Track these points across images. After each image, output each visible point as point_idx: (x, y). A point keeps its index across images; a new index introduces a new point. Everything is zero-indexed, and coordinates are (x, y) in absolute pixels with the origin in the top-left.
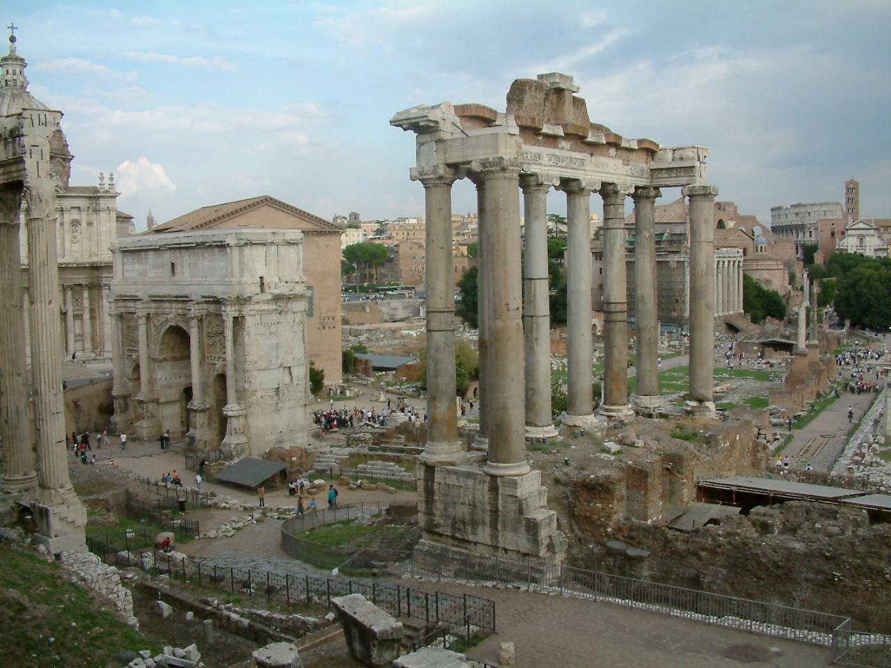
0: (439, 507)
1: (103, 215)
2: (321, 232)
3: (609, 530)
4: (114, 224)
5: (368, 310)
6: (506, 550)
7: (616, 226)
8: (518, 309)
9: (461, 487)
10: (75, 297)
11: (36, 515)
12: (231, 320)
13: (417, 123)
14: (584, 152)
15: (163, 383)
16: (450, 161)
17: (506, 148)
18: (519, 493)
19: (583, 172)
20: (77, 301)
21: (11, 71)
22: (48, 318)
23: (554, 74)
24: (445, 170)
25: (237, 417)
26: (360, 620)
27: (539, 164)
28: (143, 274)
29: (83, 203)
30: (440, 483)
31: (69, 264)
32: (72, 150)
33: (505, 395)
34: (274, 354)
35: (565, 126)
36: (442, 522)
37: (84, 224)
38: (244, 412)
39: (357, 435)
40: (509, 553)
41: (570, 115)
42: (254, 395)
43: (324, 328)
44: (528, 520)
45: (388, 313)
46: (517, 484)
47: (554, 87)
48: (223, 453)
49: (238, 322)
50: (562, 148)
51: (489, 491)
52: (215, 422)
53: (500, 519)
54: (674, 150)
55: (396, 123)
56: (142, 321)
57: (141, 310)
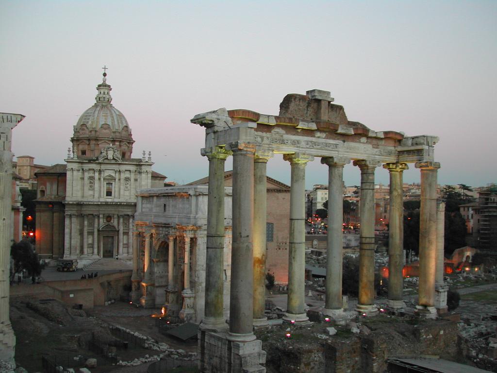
0: (207, 357)
1: (143, 175)
2: (280, 190)
4: (150, 181)
7: (367, 187)
10: (126, 222)
12: (189, 240)
14: (338, 139)
17: (246, 136)
18: (241, 353)
19: (337, 152)
20: (126, 225)
21: (102, 93)
23: (314, 90)
25: (190, 298)
27: (298, 147)
28: (151, 210)
29: (133, 168)
30: (207, 343)
32: (134, 137)
35: (318, 123)
36: (207, 367)
37: (132, 180)
38: (194, 295)
41: (325, 116)
42: (201, 285)
43: (280, 249)
44: (244, 370)
46: (239, 347)
47: (314, 98)
50: (319, 137)
51: (228, 350)
52: (180, 300)
54: (413, 138)
55: (193, 121)
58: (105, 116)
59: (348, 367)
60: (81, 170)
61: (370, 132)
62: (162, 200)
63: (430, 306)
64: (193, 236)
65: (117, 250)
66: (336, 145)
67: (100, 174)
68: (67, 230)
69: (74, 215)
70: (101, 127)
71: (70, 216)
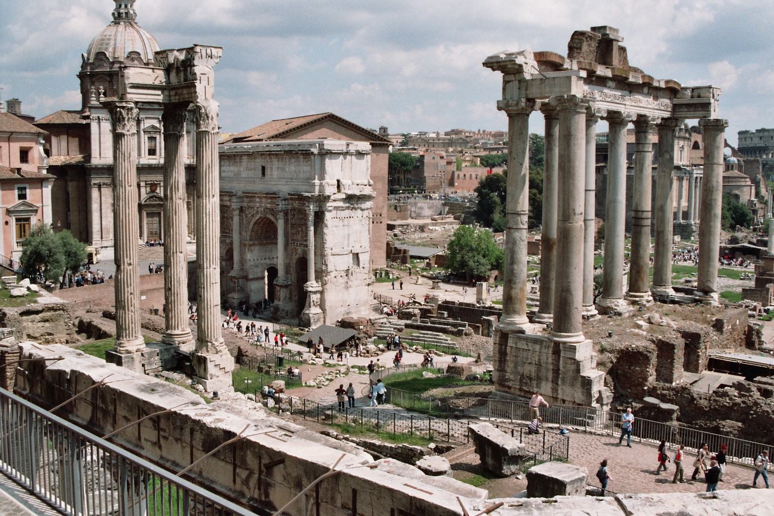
0: (510, 366)
3: (646, 388)
6: (564, 401)
8: (581, 214)
9: (529, 350)
11: (195, 362)
12: (312, 214)
14: (625, 90)
15: (252, 263)
16: (530, 96)
17: (577, 88)
18: (576, 358)
19: (624, 106)
24: (526, 103)
25: (315, 293)
26: (494, 441)
28: (238, 175)
30: (512, 347)
33: (569, 280)
34: (346, 242)
35: (613, 70)
36: (512, 377)
39: (408, 310)
40: (566, 402)
45: (415, 212)
48: (303, 321)
49: (319, 217)
51: (553, 354)
52: (295, 296)
53: (560, 376)
56: (237, 212)
57: (235, 204)
58: (132, 40)
62: (258, 160)
64: (317, 209)
68: (95, 206)
69: (104, 184)
71: (99, 187)
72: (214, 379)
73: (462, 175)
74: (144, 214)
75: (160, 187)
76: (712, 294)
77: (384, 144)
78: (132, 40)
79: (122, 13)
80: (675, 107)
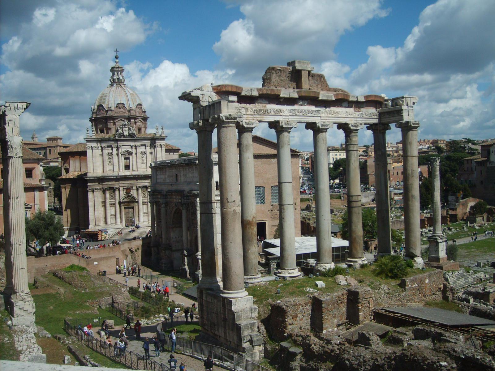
3: (286, 334)
5: (342, 198)
10: (144, 192)
13: (188, 98)
16: (205, 118)
19: (320, 118)
22: (16, 207)
27: (281, 115)
29: (148, 143)
30: (205, 300)
31: (139, 175)
33: (227, 251)
36: (207, 322)
44: (237, 324)
51: (222, 306)
55: (181, 98)
56: (163, 206)
59: (334, 317)
60: (100, 148)
61: (350, 97)
63: (417, 256)
65: (138, 219)
66: (318, 112)
67: (118, 149)
68: (90, 204)
69: (96, 189)
70: (117, 107)
71: (93, 191)
72: (20, 317)
73: (395, 173)
74: (123, 208)
75: (133, 190)
76: (415, 259)
77: (295, 154)
78: (120, 96)
79: (115, 79)
80: (381, 115)
